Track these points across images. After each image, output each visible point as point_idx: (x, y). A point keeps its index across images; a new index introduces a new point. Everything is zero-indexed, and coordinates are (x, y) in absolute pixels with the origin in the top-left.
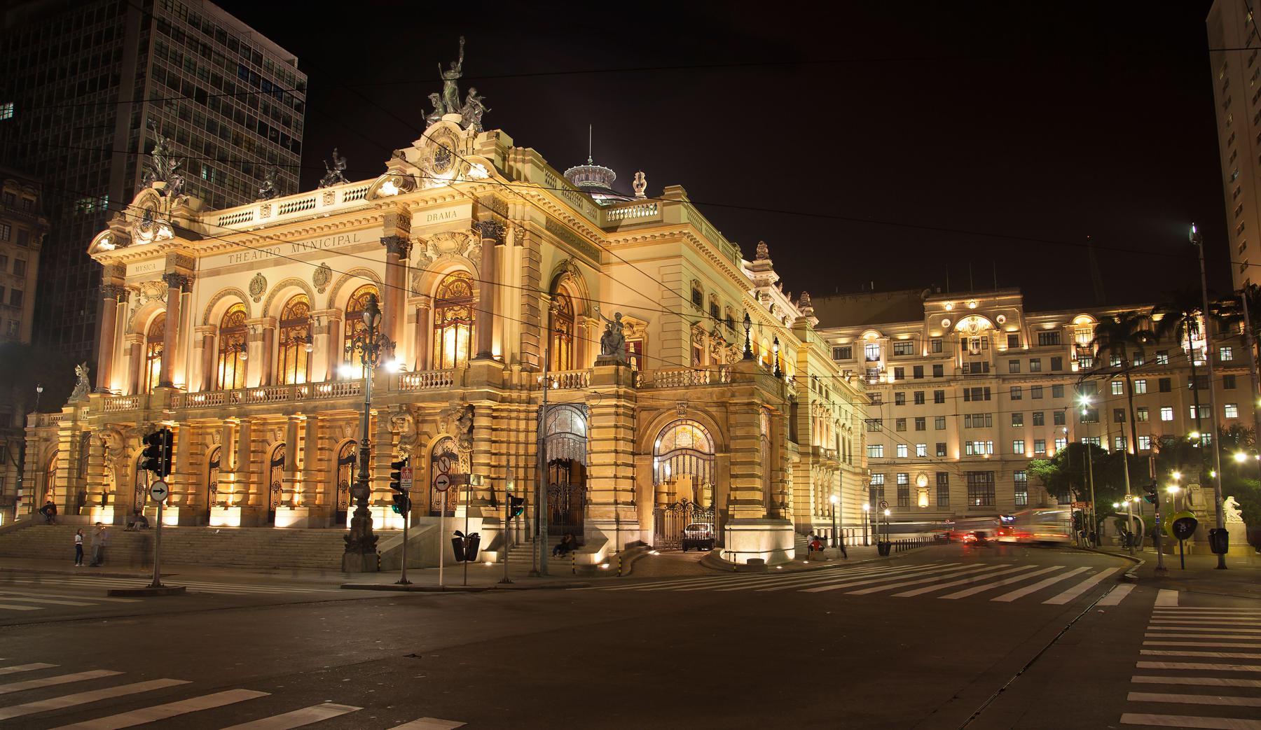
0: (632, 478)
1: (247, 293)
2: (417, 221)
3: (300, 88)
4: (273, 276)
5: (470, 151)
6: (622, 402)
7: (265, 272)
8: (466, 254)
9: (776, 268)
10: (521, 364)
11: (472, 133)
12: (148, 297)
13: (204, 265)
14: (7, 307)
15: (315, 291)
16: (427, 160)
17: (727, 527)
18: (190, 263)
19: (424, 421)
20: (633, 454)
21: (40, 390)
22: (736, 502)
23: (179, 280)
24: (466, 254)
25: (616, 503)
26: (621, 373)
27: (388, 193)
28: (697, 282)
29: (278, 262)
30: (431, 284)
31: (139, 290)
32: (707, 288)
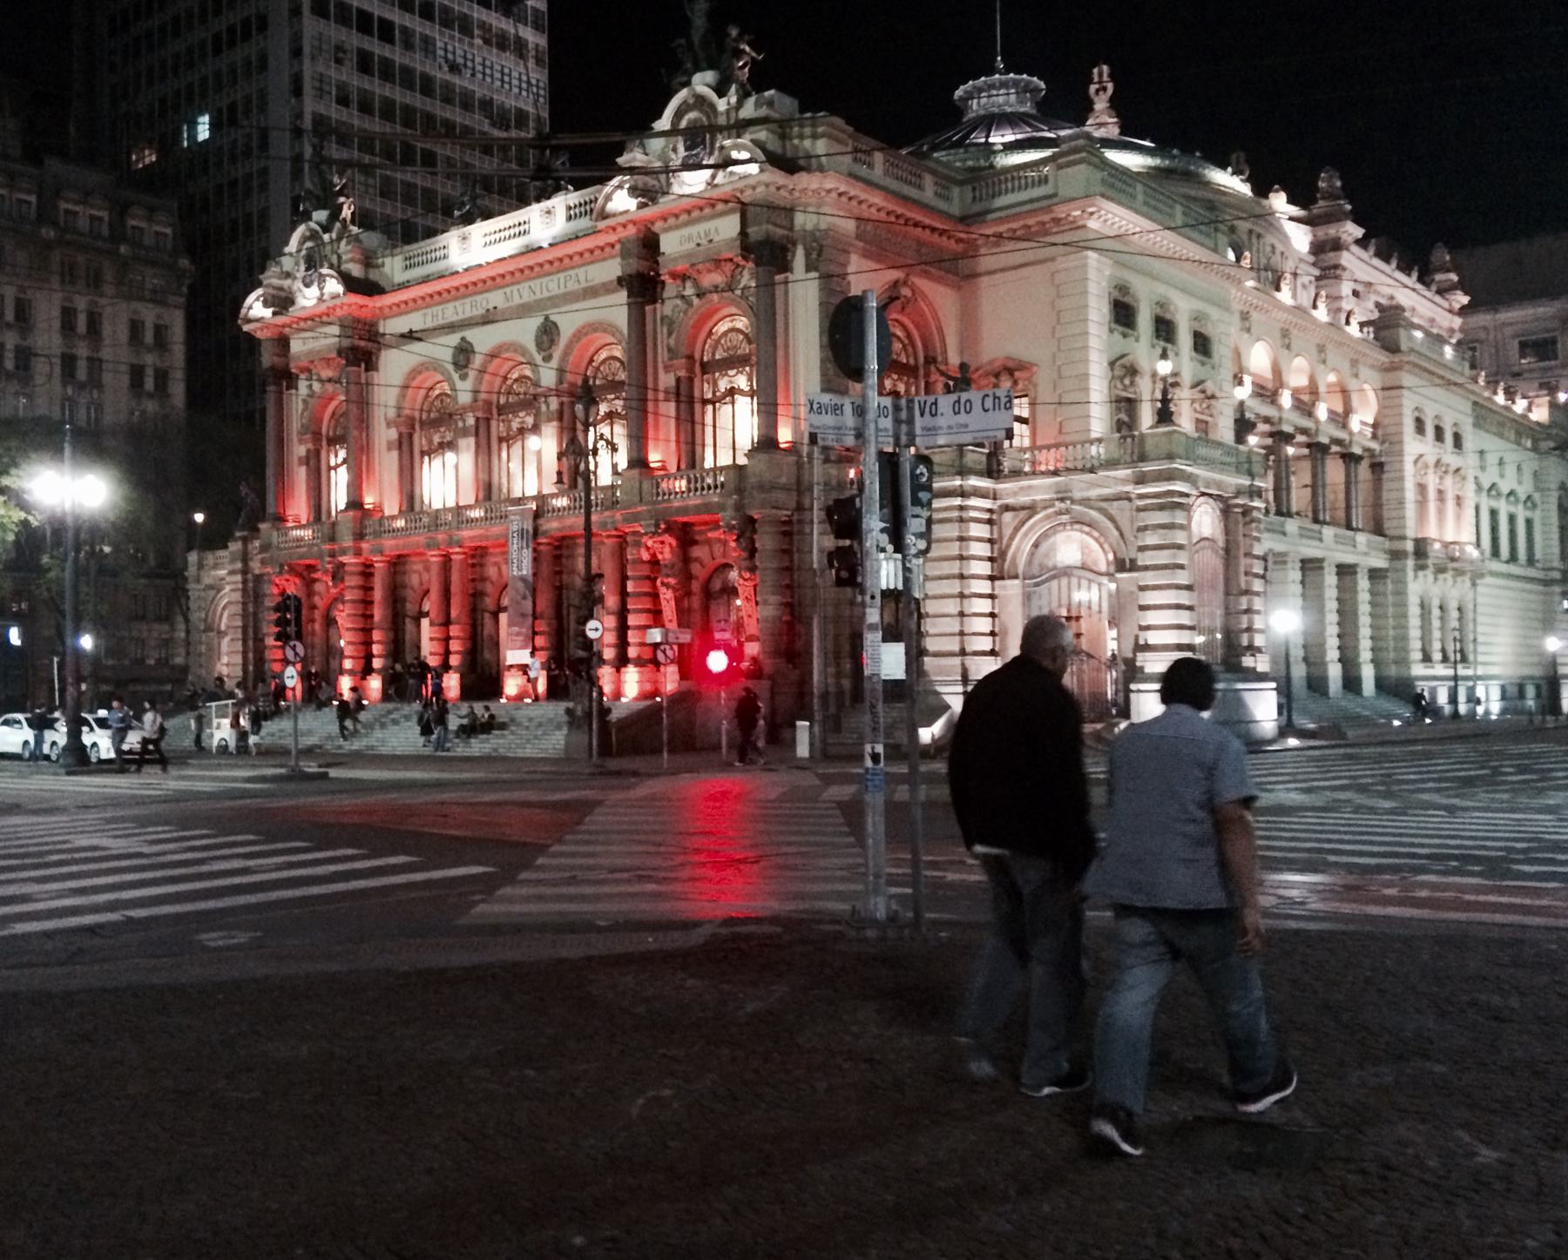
0: (992, 615)
2: (671, 244)
7: (472, 335)
8: (738, 292)
11: (734, 100)
14: (151, 396)
17: (1133, 687)
19: (695, 543)
20: (992, 578)
21: (199, 518)
25: (963, 653)
27: (621, 209)
28: (1123, 288)
29: (488, 319)
31: (309, 371)
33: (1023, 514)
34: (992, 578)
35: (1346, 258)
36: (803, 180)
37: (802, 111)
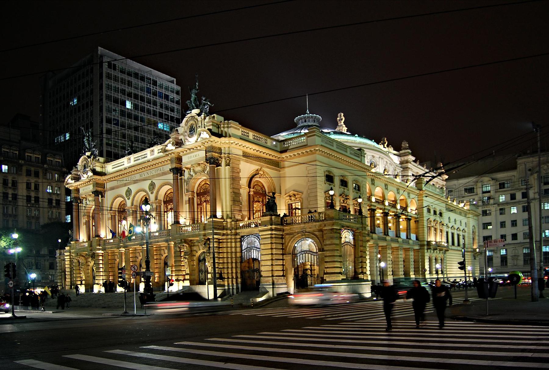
1: (125, 196)
3: (177, 93)
4: (134, 188)
5: (203, 126)
6: (274, 232)
7: (131, 187)
8: (206, 172)
9: (413, 155)
10: (231, 218)
12: (89, 201)
13: (108, 185)
15: (150, 193)
16: (186, 132)
18: (103, 186)
20: (283, 254)
22: (327, 273)
23: (99, 193)
24: (206, 172)
26: (273, 219)
29: (136, 182)
30: (194, 186)
32: (337, 173)
33: (292, 236)
34: (283, 254)
35: (409, 165)
36: (223, 140)
37: (225, 120)
